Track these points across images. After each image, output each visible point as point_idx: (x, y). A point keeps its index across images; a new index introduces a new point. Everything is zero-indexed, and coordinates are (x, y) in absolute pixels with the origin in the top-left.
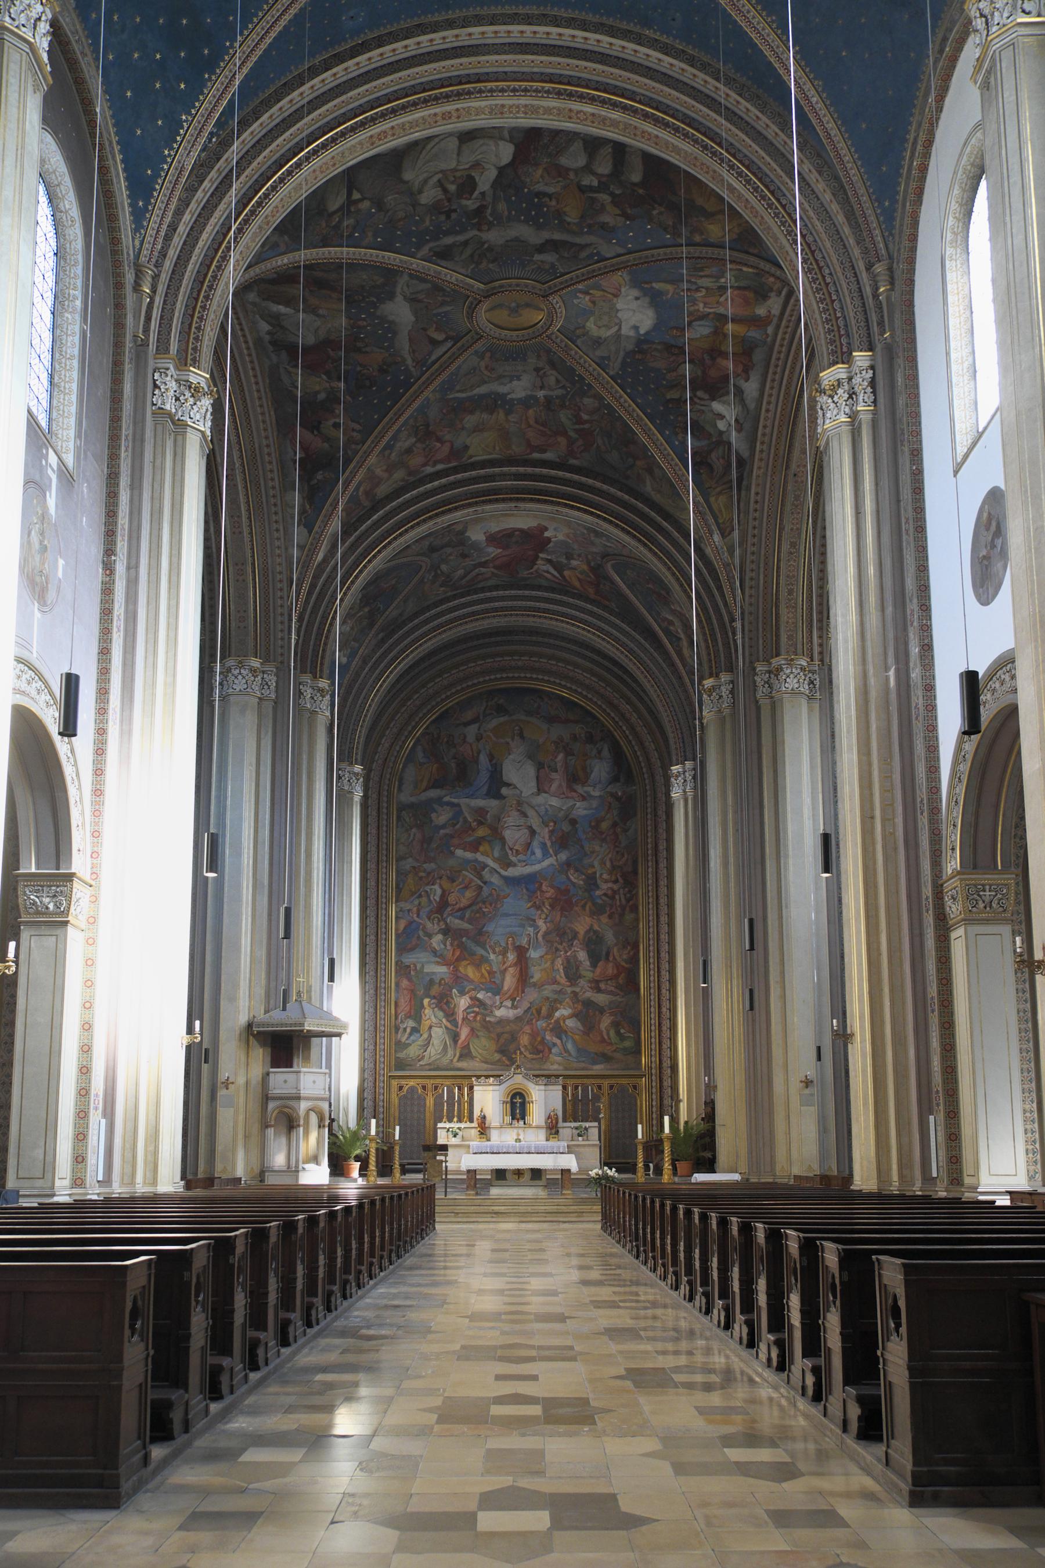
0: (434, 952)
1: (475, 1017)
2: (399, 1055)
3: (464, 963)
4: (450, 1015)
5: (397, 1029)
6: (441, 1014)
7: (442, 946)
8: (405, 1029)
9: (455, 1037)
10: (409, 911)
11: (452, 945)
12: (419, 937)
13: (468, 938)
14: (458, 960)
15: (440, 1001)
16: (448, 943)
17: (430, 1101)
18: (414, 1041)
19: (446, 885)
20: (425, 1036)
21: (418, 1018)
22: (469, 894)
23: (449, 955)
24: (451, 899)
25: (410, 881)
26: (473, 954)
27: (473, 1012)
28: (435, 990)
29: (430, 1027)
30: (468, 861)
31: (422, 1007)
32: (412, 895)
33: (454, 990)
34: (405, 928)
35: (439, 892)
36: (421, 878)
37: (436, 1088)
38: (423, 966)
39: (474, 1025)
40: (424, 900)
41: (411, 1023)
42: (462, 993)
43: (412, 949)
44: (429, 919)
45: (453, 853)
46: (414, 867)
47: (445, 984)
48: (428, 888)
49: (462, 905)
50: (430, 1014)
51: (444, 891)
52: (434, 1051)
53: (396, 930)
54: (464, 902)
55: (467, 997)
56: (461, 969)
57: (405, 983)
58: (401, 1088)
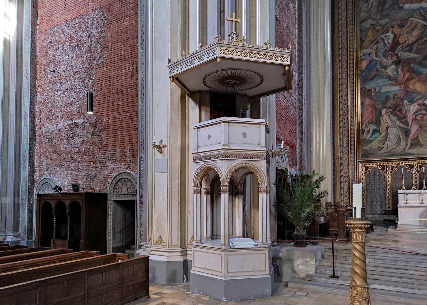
0: (389, 78)
1: (423, 117)
2: (365, 148)
3: (413, 81)
4: (403, 118)
5: (363, 131)
6: (395, 118)
7: (395, 73)
8: (369, 131)
9: (407, 133)
10: (369, 54)
11: (402, 70)
12: (377, 70)
13: (416, 64)
14: (408, 80)
15: (394, 110)
16: (400, 70)
17: (389, 177)
18: (375, 138)
19: (397, 30)
20: (384, 134)
21: (378, 122)
22: (415, 33)
23: (400, 78)
24: (401, 40)
25: (370, 34)
26: (419, 74)
27: (422, 114)
28: (391, 103)
29: (387, 128)
30: (414, 10)
31: (381, 115)
32: (372, 43)
33: (405, 101)
34: (367, 65)
35: (392, 36)
36: (378, 31)
37: (393, 168)
38: (381, 88)
39: (422, 123)
40: (381, 44)
41: (373, 127)
42: (411, 102)
43: (372, 79)
44: (384, 56)
45: (402, 8)
46: (372, 25)
47: (398, 98)
48: (383, 36)
49: (410, 42)
50: (386, 119)
51: (395, 35)
52: (390, 144)
53: (361, 68)
54: (412, 39)
55: (416, 105)
56: (411, 86)
57: (367, 101)
58: (367, 169)
